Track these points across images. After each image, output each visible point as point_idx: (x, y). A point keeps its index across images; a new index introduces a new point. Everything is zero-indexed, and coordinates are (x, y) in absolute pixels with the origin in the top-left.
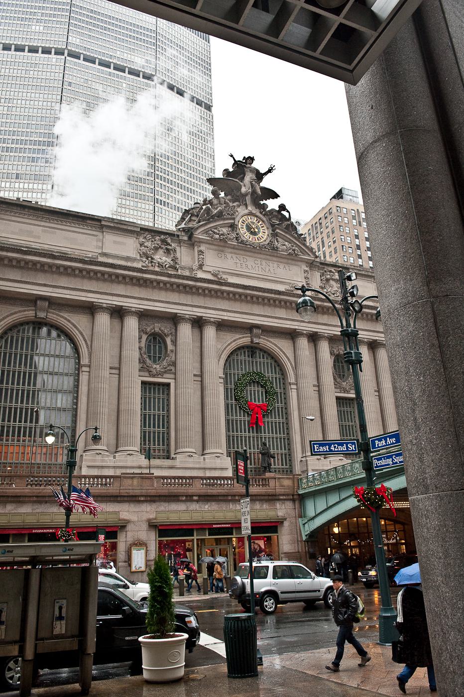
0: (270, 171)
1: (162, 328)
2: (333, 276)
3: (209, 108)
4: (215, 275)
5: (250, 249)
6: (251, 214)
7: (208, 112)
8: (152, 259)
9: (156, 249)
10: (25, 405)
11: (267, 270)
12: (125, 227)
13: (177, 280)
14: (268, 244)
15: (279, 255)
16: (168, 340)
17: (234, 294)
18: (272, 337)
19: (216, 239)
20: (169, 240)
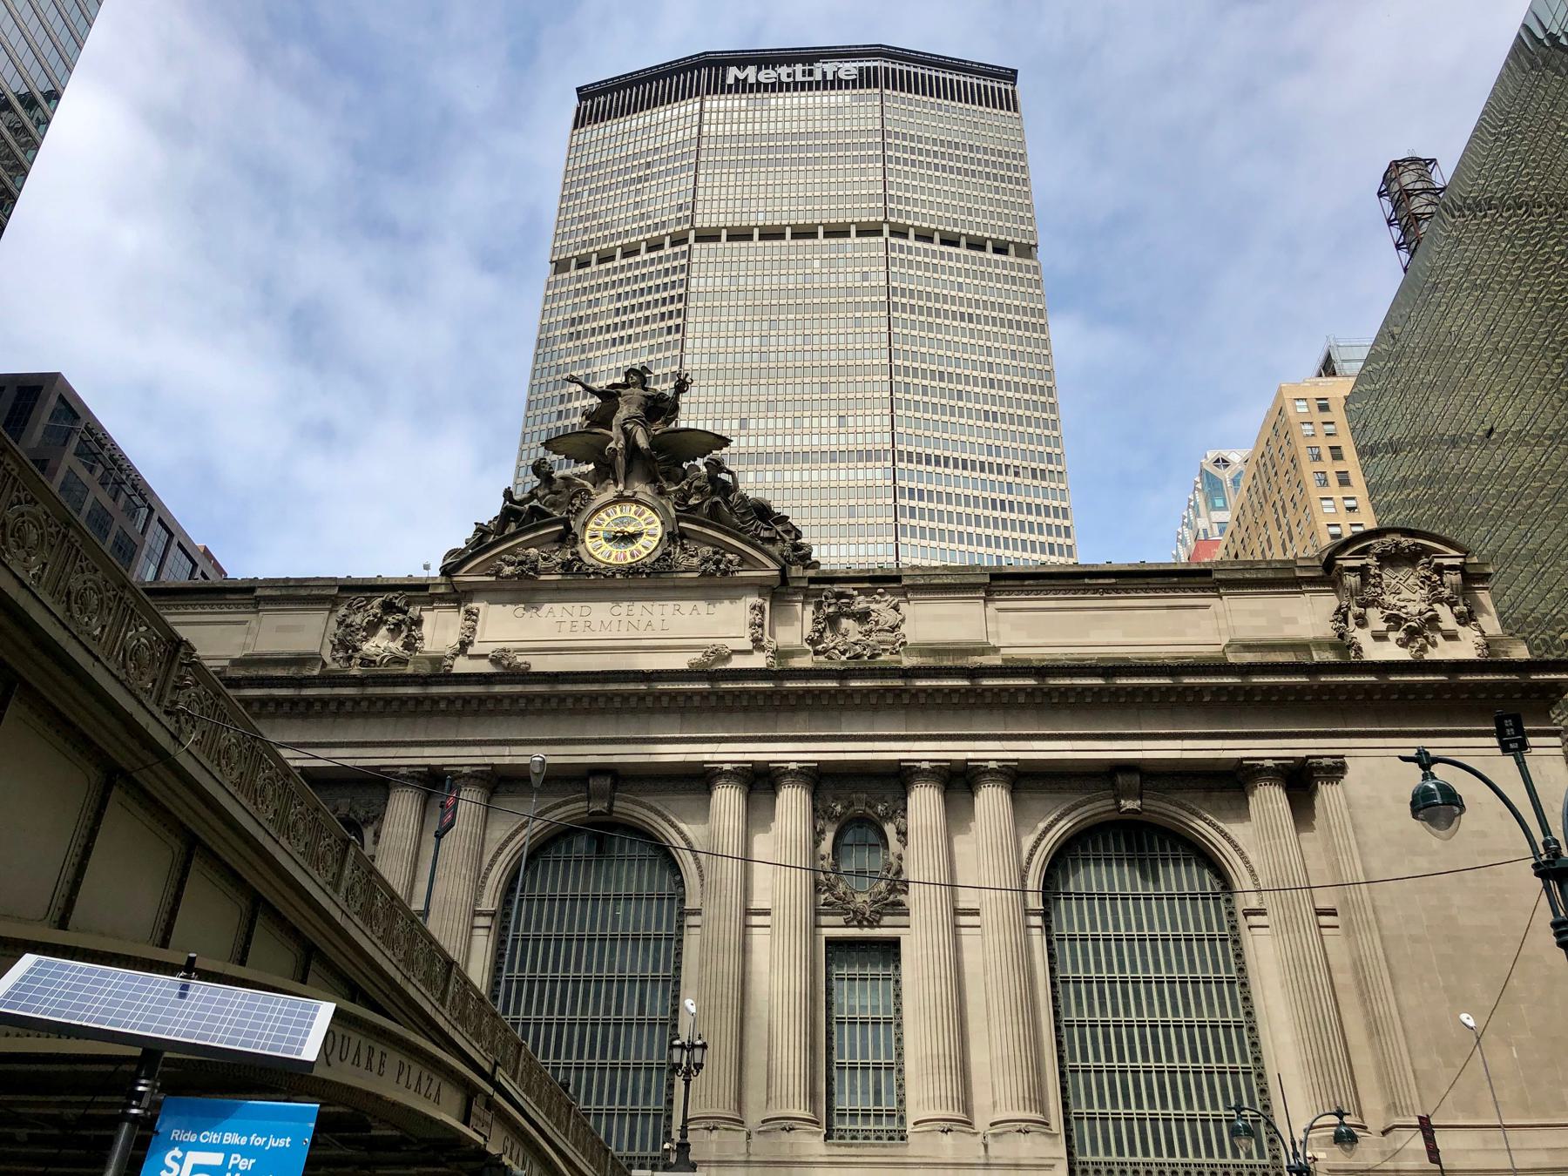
0: (682, 386)
1: (356, 807)
2: (848, 605)
3: (1026, 251)
4: (495, 661)
5: (599, 584)
6: (621, 499)
7: (1027, 262)
8: (356, 650)
9: (372, 628)
10: (556, 1016)
11: (643, 625)
12: (303, 592)
13: (378, 691)
14: (658, 560)
15: (677, 583)
16: (368, 834)
17: (530, 698)
18: (649, 793)
19: (507, 577)
20: (400, 603)
